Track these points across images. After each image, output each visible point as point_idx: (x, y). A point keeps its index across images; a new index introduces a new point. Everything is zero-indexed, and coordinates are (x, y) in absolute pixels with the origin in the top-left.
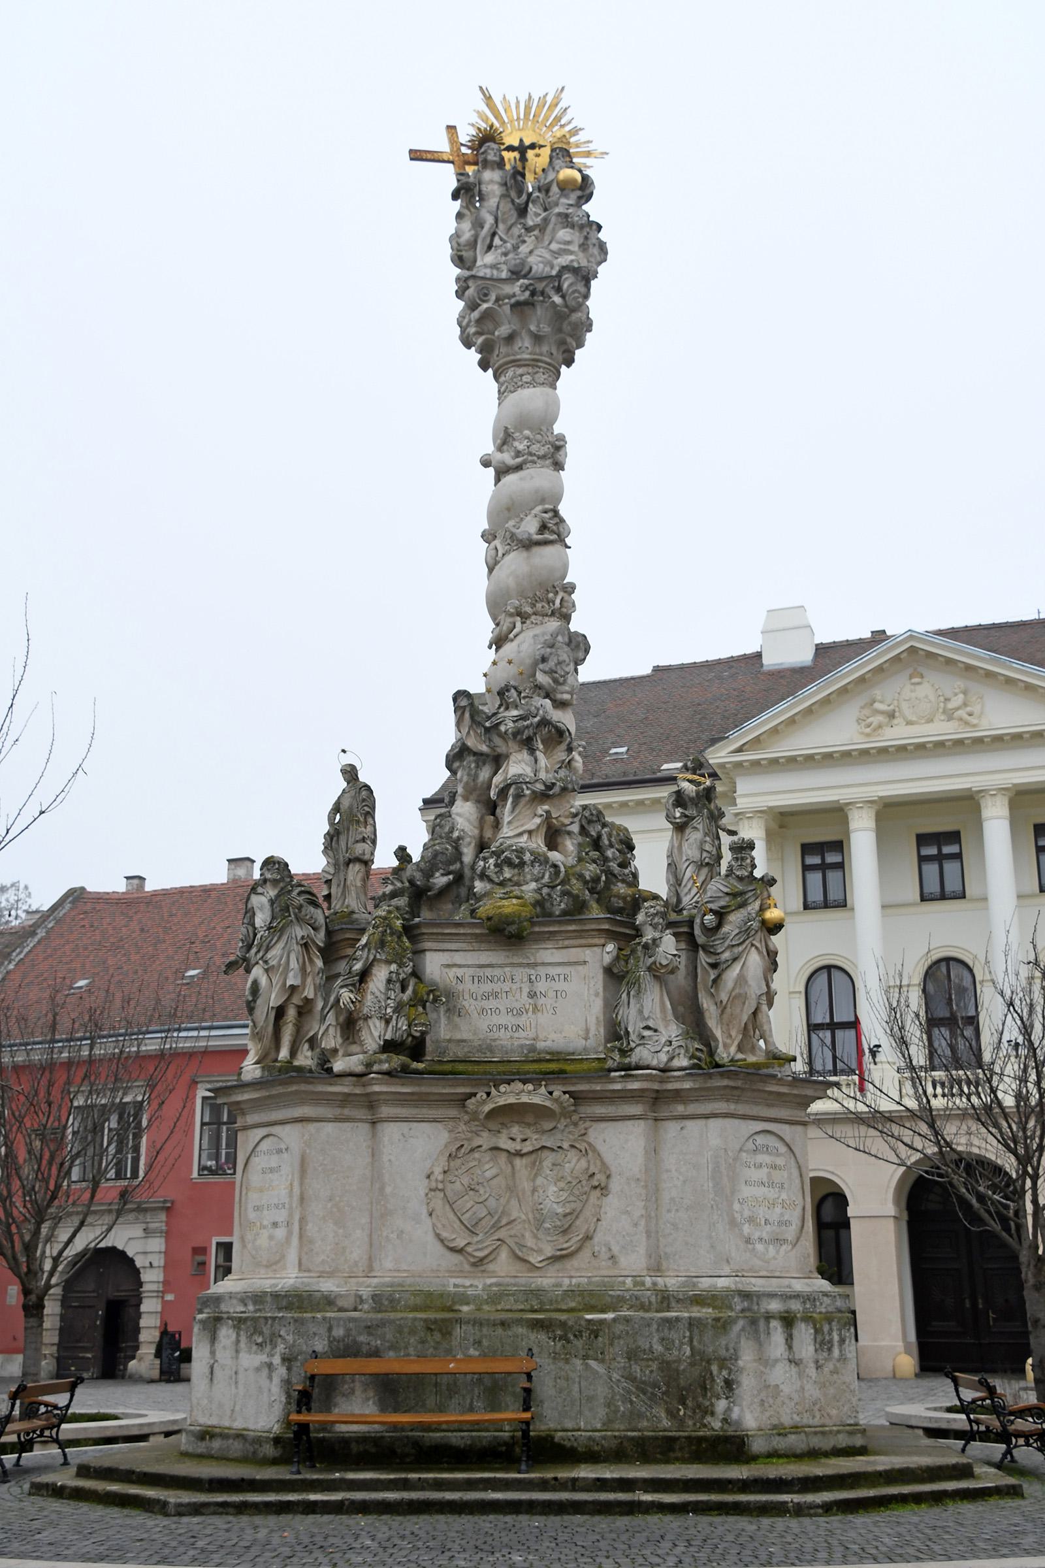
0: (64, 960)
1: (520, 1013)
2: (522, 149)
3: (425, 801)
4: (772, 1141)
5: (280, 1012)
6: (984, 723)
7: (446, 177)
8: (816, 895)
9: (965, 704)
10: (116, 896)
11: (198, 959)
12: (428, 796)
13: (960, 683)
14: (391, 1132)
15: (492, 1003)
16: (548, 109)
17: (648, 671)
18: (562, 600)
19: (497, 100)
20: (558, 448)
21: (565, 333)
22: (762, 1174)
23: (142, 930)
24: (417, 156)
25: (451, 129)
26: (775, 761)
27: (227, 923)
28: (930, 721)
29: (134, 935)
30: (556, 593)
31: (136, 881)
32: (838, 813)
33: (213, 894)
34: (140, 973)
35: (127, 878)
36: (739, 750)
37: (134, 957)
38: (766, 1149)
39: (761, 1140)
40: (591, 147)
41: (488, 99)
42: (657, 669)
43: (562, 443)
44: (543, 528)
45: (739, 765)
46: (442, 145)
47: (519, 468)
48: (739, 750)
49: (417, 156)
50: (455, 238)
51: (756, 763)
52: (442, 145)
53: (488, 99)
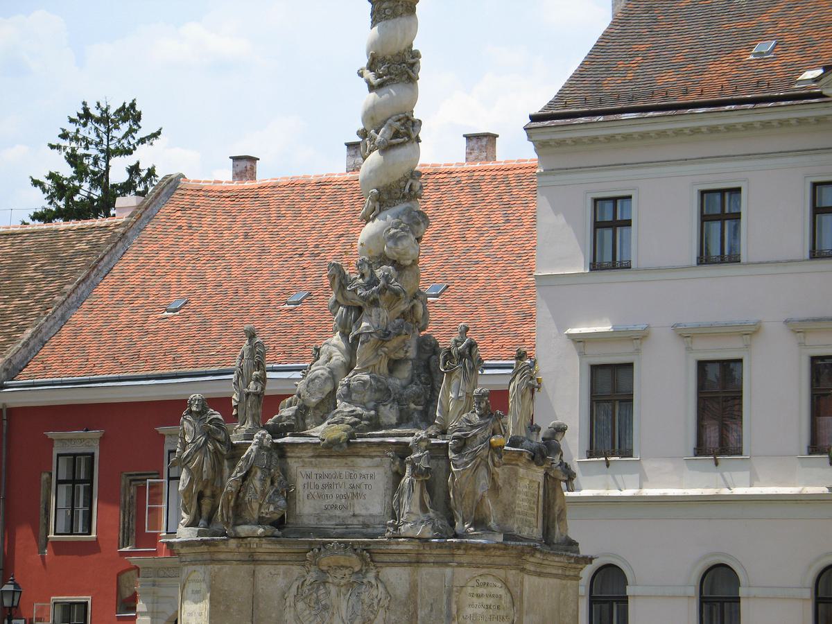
0: (160, 271)
3: (534, 118)
4: (490, 580)
5: (201, 496)
10: (218, 187)
12: (536, 109)
14: (264, 570)
15: (326, 491)
18: (411, 185)
20: (413, 65)
23: (246, 236)
27: (340, 230)
29: (237, 241)
30: (406, 182)
31: (243, 164)
34: (241, 293)
35: (235, 159)
37: (236, 272)
38: (486, 585)
43: (414, 60)
44: (396, 134)
47: (381, 86)
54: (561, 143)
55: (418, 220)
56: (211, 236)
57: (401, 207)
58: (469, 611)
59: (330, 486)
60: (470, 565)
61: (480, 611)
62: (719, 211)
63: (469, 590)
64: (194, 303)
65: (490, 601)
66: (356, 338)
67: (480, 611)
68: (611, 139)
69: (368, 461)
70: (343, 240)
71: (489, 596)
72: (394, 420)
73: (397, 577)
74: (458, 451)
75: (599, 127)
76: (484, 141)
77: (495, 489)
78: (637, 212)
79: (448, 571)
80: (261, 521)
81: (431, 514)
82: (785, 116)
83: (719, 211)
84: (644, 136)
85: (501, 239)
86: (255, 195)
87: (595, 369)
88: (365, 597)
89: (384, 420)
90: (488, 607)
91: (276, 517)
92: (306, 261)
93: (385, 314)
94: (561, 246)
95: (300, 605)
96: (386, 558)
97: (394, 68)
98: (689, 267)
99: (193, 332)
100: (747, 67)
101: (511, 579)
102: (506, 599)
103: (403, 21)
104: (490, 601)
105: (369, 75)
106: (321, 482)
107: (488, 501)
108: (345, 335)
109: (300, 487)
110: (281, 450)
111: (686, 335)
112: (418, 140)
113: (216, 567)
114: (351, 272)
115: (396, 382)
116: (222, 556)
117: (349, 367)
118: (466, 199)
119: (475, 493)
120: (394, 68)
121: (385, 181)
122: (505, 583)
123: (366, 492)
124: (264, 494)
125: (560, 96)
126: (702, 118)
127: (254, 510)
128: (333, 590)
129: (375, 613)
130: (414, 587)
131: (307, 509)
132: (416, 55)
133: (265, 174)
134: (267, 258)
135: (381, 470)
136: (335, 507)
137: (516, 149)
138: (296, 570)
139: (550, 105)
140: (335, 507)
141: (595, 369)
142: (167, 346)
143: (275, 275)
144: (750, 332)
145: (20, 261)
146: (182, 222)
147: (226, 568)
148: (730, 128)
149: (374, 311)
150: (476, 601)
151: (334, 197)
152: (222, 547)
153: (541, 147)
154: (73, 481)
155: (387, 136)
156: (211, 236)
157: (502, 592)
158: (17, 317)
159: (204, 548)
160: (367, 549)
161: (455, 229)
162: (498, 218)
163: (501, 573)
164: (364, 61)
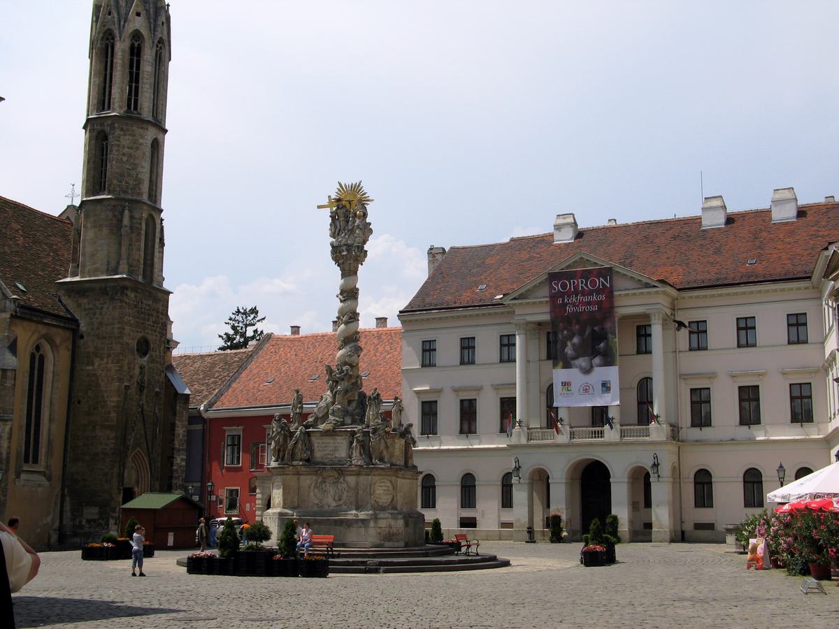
2: (350, 202)
3: (400, 312)
4: (385, 481)
5: (279, 450)
7: (327, 212)
10: (285, 337)
11: (317, 370)
12: (401, 309)
14: (302, 478)
15: (325, 449)
16: (356, 188)
17: (506, 240)
21: (360, 255)
23: (296, 355)
24: (319, 207)
25: (329, 197)
26: (528, 303)
27: (330, 353)
31: (295, 329)
33: (326, 338)
35: (292, 327)
36: (515, 299)
37: (292, 368)
38: (384, 482)
39: (382, 481)
40: (369, 198)
41: (341, 185)
42: (512, 240)
44: (350, 318)
45: (514, 305)
46: (326, 202)
48: (515, 299)
49: (319, 207)
50: (331, 230)
51: (520, 304)
53: (341, 185)
54: (410, 321)
55: (358, 350)
56: (283, 355)
57: (352, 344)
58: (378, 492)
59: (326, 446)
60: (378, 475)
61: (382, 492)
62: (468, 345)
63: (378, 484)
64: (277, 380)
65: (385, 488)
66: (336, 392)
67: (382, 492)
68: (428, 319)
69: (340, 438)
70: (331, 356)
71: (385, 486)
72: (350, 422)
73: (351, 480)
74: (373, 433)
75: (424, 315)
76: (383, 320)
77: (387, 447)
78: (438, 346)
79: (370, 477)
80: (301, 460)
81: (364, 456)
82: (490, 311)
83: (468, 345)
84: (440, 318)
85: (389, 356)
86: (299, 340)
87: (424, 403)
88: (339, 487)
89: (346, 422)
90: (385, 490)
91: (307, 458)
92: (318, 364)
93: (346, 383)
94: (411, 359)
95: (316, 490)
96: (347, 473)
97: (349, 294)
98: (457, 366)
99: (277, 390)
100: (477, 294)
101: (393, 480)
102: (391, 488)
103: (352, 278)
104: (385, 488)
105: (340, 297)
106: (323, 446)
107: (385, 452)
108: (332, 391)
109: (315, 448)
110: (309, 434)
111: (456, 390)
112: (358, 320)
113: (284, 477)
114: (334, 368)
115: (350, 408)
116: (287, 473)
117: (333, 403)
118: (376, 341)
119: (379, 449)
120: (349, 294)
121: (346, 335)
122: (391, 482)
123: (340, 448)
124: (302, 450)
125: (410, 304)
126: (461, 312)
127: (299, 456)
128: (328, 484)
129: (343, 493)
130: (357, 483)
131: (318, 455)
132: (358, 289)
133: (303, 333)
134: (304, 363)
135: (345, 441)
136: (328, 454)
137: (394, 323)
138: (314, 477)
139: (406, 308)
140: (328, 454)
141: (424, 403)
142: (267, 396)
143: (306, 369)
144: (479, 389)
145: (213, 365)
146: (272, 350)
147: (289, 477)
148: (471, 316)
149: (342, 383)
150: (380, 488)
151: (328, 341)
152: (288, 469)
153: (403, 322)
154: (233, 445)
155: (347, 319)
156: (283, 355)
157: (390, 485)
158: (212, 385)
159: (280, 470)
160: (340, 469)
161: (372, 352)
162: (388, 348)
163: (389, 478)
164: (339, 292)
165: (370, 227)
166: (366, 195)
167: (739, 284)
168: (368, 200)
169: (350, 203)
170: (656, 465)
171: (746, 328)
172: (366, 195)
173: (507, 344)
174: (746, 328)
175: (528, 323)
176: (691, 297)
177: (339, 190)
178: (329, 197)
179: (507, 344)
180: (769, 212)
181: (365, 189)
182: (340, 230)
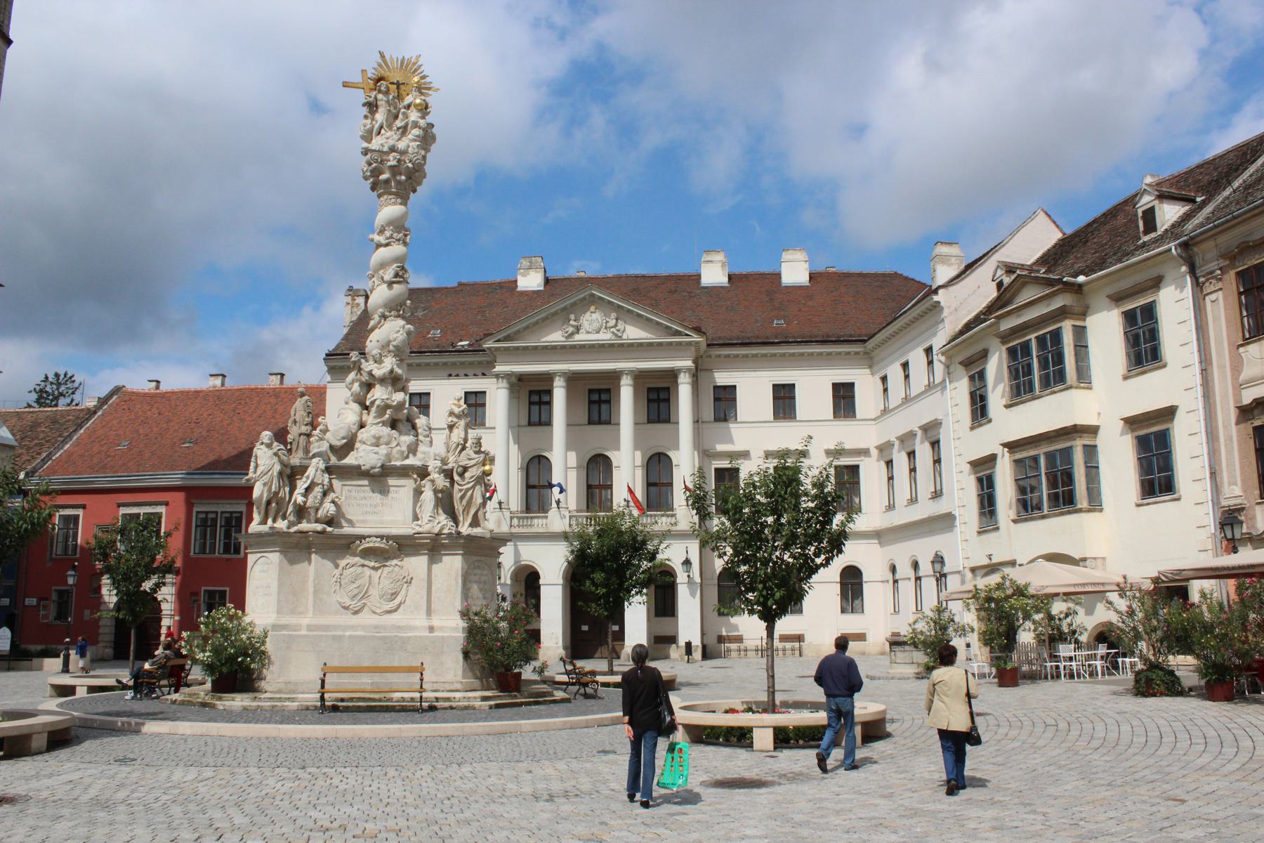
1: (375, 506)
5: (269, 503)
6: (625, 337)
7: (360, 96)
8: (535, 418)
9: (616, 325)
13: (614, 315)
15: (364, 502)
19: (388, 58)
22: (476, 578)
25: (364, 71)
26: (517, 348)
28: (598, 332)
32: (548, 378)
41: (382, 55)
42: (460, 284)
44: (396, 275)
45: (498, 349)
47: (387, 245)
49: (346, 85)
52: (358, 79)
53: (382, 55)
118: (273, 400)
133: (163, 388)
148: (427, 365)
165: (434, 130)
166: (428, 80)
167: (773, 344)
168: (429, 89)
169: (398, 88)
170: (687, 562)
171: (784, 399)
172: (428, 80)
173: (475, 401)
174: (784, 399)
175: (507, 376)
176: (719, 356)
177: (380, 65)
178: (364, 71)
179: (475, 401)
180: (778, 275)
181: (426, 70)
182: (381, 127)
